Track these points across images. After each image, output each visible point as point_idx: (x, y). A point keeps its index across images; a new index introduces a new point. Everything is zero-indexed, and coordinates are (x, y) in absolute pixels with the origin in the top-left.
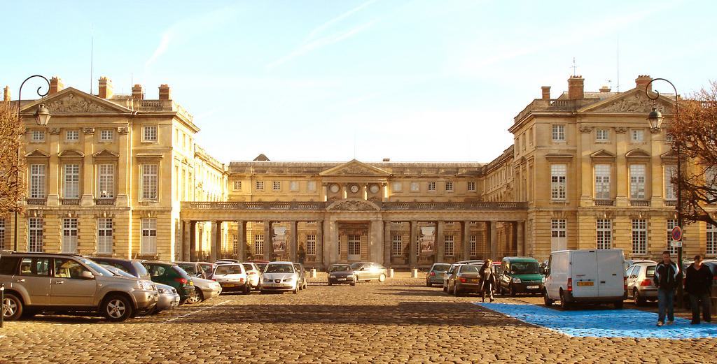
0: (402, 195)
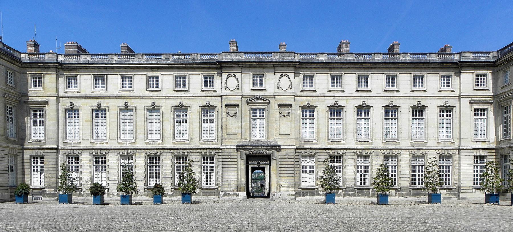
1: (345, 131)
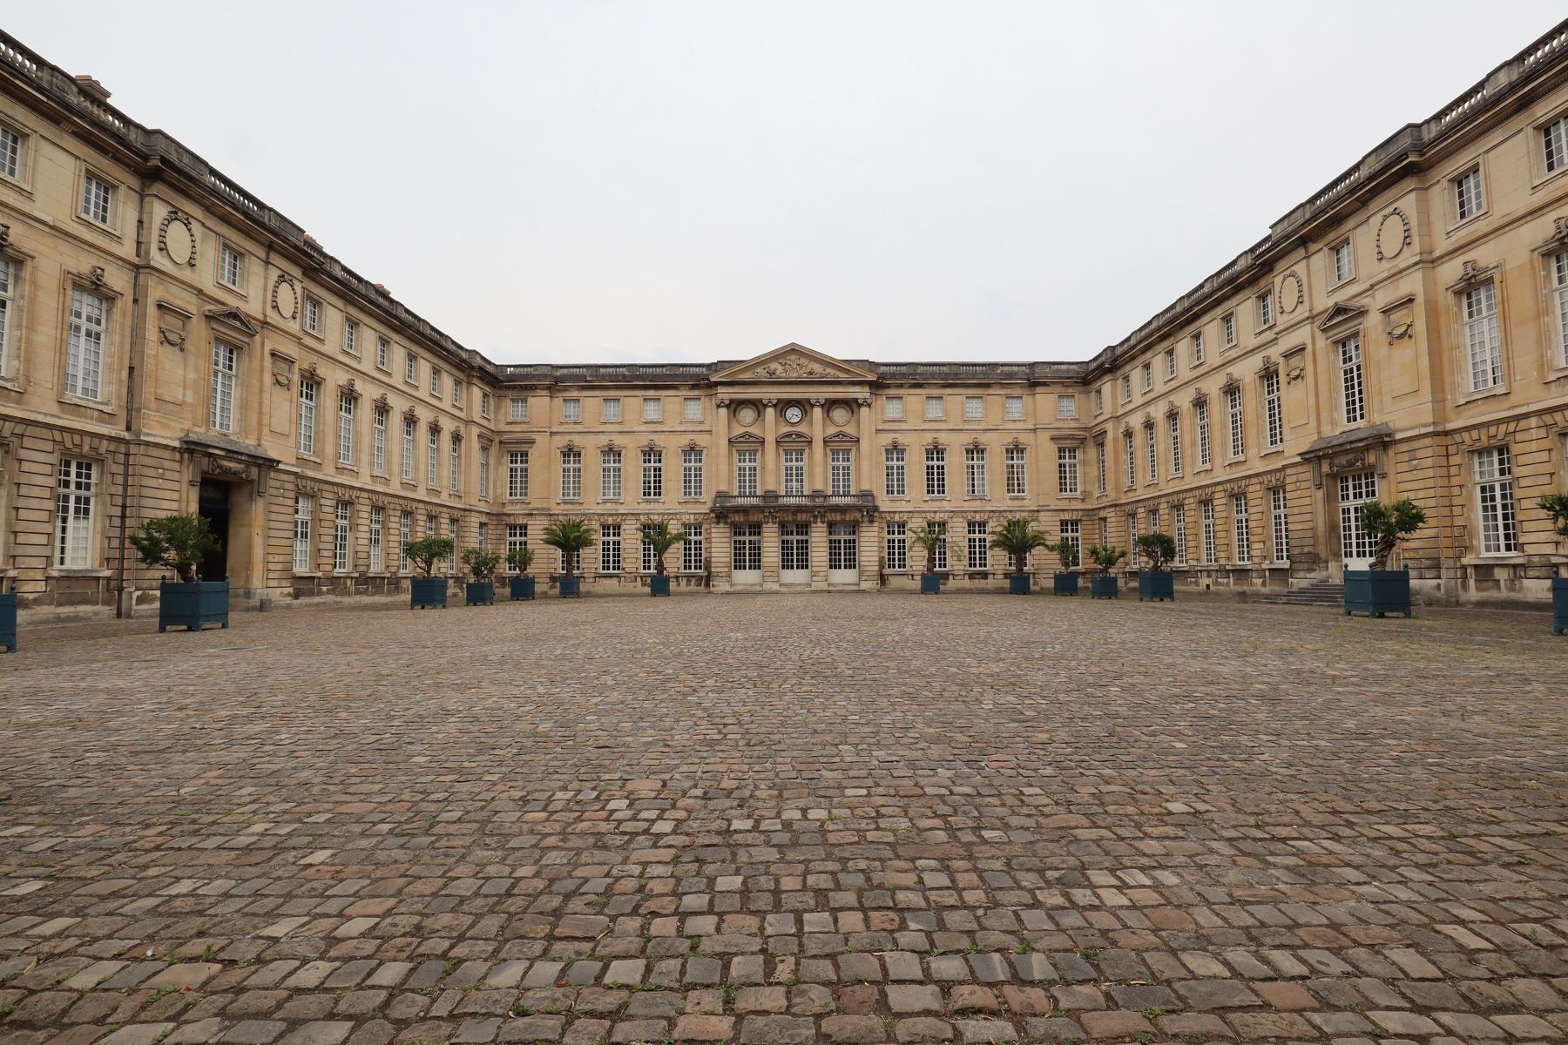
0: (904, 426)
1: (357, 450)
